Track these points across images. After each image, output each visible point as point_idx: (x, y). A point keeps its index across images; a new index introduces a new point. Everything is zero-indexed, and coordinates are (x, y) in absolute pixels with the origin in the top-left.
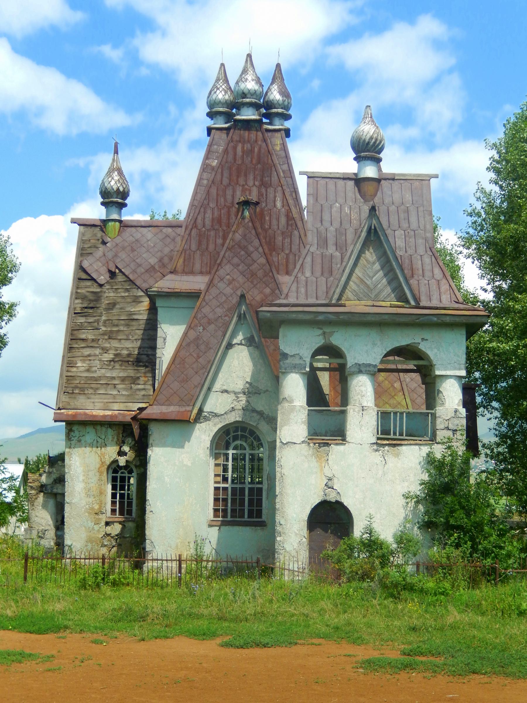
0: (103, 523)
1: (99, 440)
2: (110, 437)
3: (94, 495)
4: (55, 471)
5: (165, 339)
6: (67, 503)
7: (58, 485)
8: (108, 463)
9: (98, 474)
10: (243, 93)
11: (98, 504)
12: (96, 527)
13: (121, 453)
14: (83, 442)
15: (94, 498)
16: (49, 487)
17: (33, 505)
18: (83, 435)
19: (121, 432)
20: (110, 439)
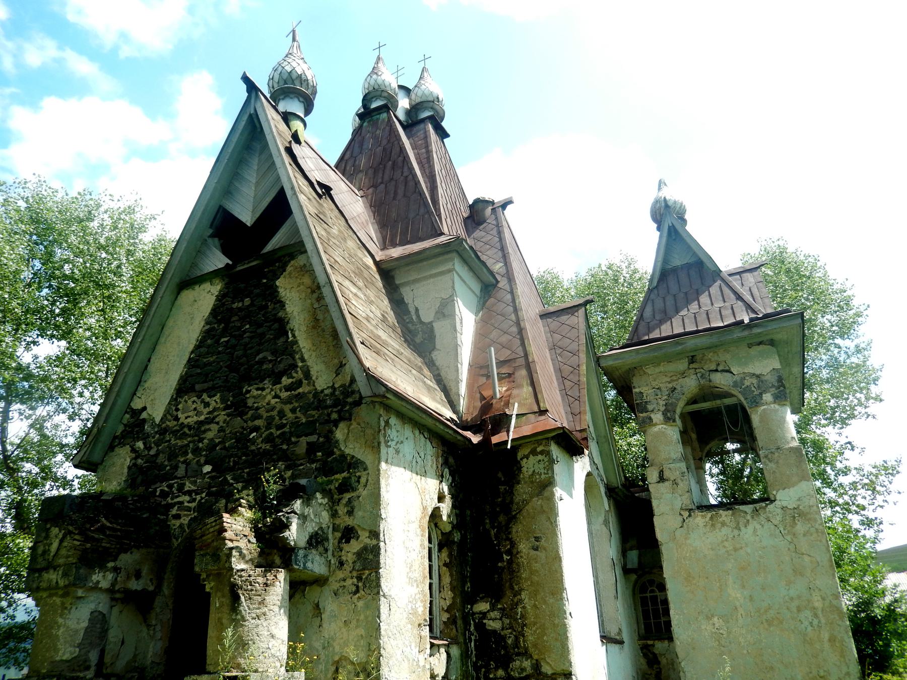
0: (428, 651)
1: (419, 460)
2: (429, 457)
3: (416, 581)
4: (312, 516)
5: (461, 323)
6: (384, 596)
7: (314, 551)
8: (430, 511)
9: (419, 531)
10: (438, 98)
11: (422, 601)
12: (421, 657)
13: (441, 498)
14: (401, 455)
15: (417, 586)
16: (301, 553)
17: (262, 603)
18: (402, 442)
19: (440, 452)
20: (430, 464)
